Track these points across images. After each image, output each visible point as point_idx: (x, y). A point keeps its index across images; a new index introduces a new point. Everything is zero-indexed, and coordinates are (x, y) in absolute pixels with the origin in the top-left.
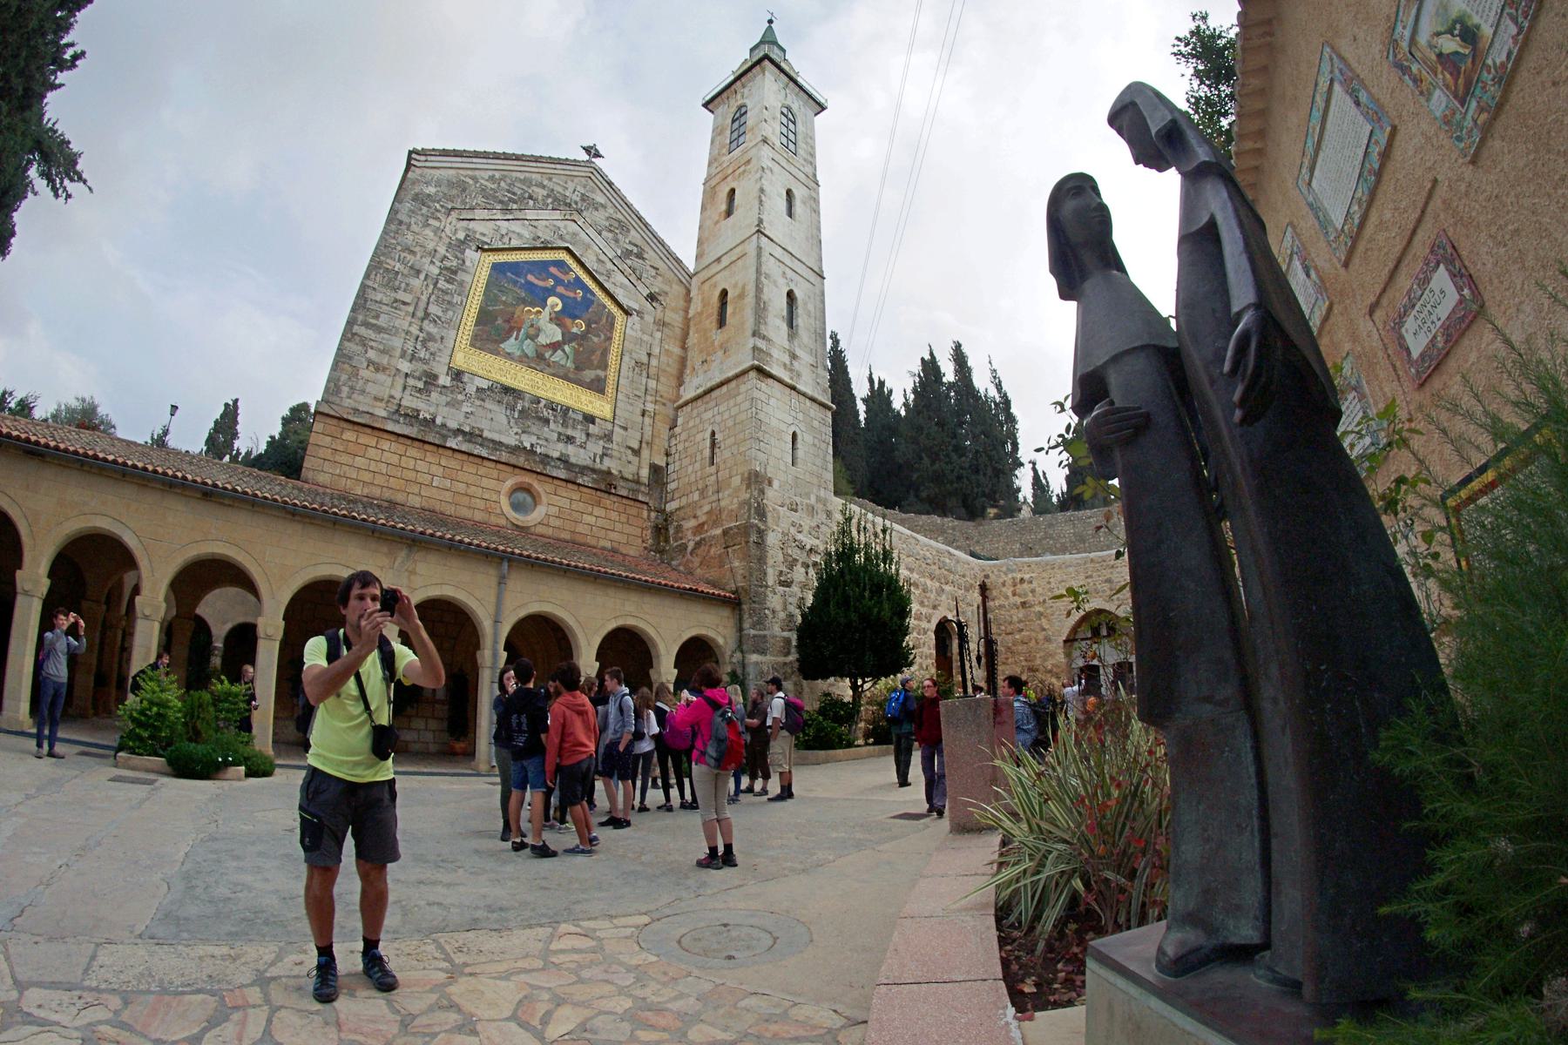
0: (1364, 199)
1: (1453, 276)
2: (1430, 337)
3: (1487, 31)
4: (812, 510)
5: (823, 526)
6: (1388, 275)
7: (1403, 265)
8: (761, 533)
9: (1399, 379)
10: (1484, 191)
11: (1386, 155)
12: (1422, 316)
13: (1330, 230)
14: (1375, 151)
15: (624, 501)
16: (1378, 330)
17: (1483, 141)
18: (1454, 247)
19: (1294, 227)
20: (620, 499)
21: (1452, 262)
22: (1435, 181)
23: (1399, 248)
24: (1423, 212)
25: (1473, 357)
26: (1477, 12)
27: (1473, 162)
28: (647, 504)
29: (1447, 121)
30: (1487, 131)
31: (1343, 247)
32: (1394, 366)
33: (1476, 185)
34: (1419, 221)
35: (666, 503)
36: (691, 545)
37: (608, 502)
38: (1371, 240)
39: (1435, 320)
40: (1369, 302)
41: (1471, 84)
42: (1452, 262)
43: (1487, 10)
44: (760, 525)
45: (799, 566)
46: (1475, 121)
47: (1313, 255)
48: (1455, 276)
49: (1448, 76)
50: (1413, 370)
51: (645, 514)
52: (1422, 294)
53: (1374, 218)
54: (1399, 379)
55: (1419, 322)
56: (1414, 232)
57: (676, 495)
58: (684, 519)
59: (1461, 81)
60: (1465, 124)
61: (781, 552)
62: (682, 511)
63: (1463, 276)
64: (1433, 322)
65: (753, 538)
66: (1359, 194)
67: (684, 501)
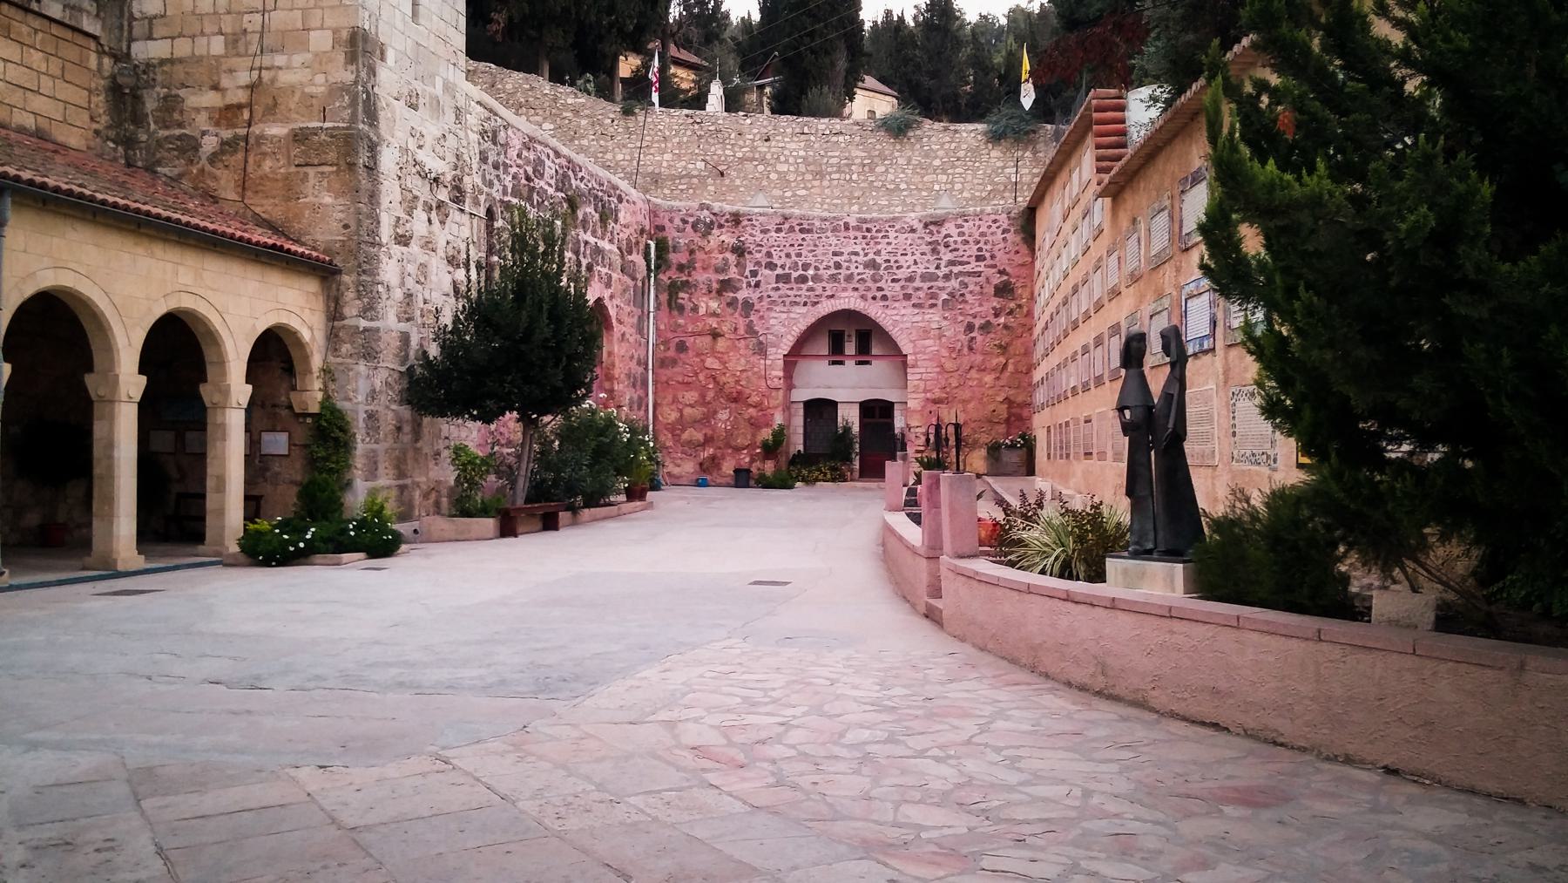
4: (436, 105)
5: (450, 137)
8: (373, 148)
15: (55, 30)
20: (46, 23)
28: (95, 38)
35: (131, 40)
36: (209, 144)
37: (25, 29)
44: (372, 135)
45: (420, 208)
51: (93, 61)
57: (159, 31)
58: (184, 86)
61: (397, 182)
62: (178, 68)
65: (363, 158)
67: (183, 48)
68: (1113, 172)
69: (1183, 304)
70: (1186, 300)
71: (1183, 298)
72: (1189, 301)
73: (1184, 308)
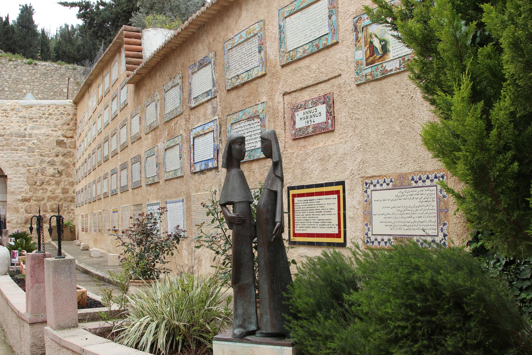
0: (307, 52)
1: (327, 112)
2: (307, 125)
3: (391, 55)
6: (300, 88)
7: (309, 89)
9: (285, 129)
10: (355, 97)
11: (327, 47)
12: (307, 115)
13: (283, 45)
14: (323, 42)
16: (284, 103)
17: (364, 83)
18: (333, 102)
19: (264, 24)
21: (330, 107)
22: (340, 75)
23: (311, 83)
24: (329, 80)
25: (321, 145)
26: (393, 47)
27: (358, 85)
29: (358, 63)
30: (368, 82)
31: (285, 59)
32: (285, 123)
33: (353, 93)
34: (325, 81)
38: (300, 68)
39: (312, 121)
40: (286, 90)
41: (374, 63)
42: (330, 107)
43: (396, 51)
46: (366, 76)
47: (267, 45)
48: (328, 112)
49: (368, 52)
50: (293, 132)
52: (312, 107)
53: (306, 62)
54: (285, 129)
55: (305, 116)
56: (321, 83)
59: (371, 58)
60: (363, 72)
63: (331, 114)
64: (310, 121)
66: (307, 47)
68: (140, 66)
69: (192, 140)
70: (194, 138)
71: (192, 137)
72: (196, 140)
73: (192, 143)
